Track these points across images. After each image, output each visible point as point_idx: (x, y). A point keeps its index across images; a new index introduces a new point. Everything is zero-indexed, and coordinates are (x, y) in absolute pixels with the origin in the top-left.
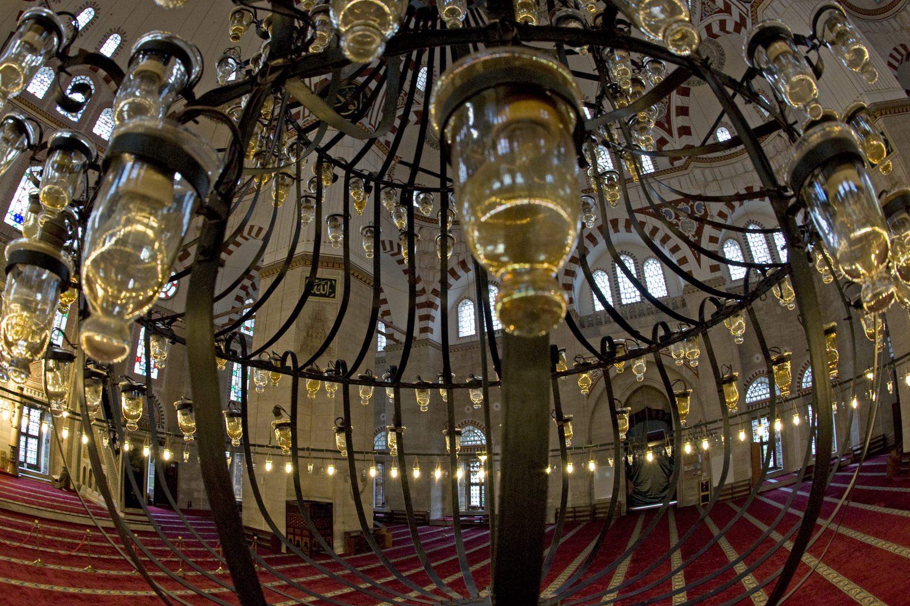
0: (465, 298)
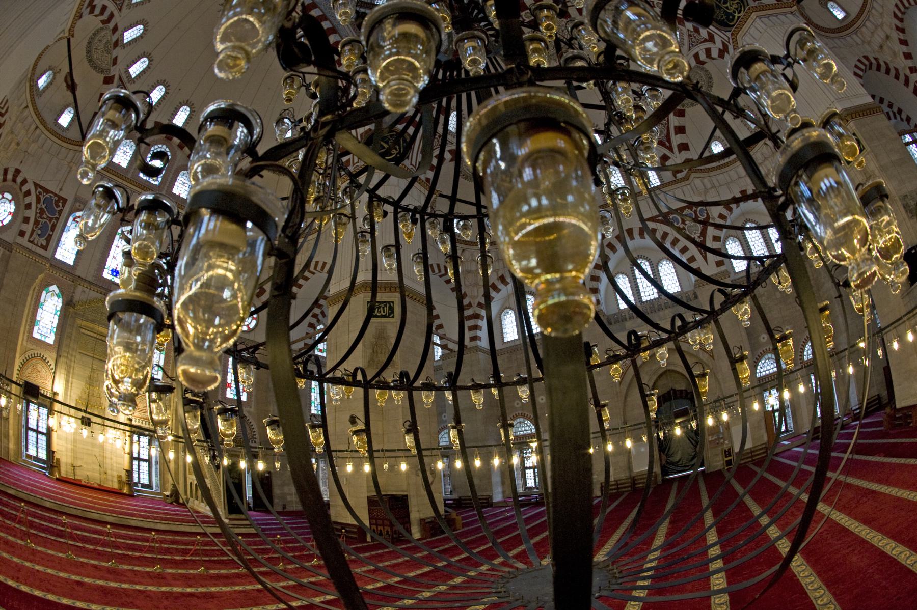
0: (507, 308)
